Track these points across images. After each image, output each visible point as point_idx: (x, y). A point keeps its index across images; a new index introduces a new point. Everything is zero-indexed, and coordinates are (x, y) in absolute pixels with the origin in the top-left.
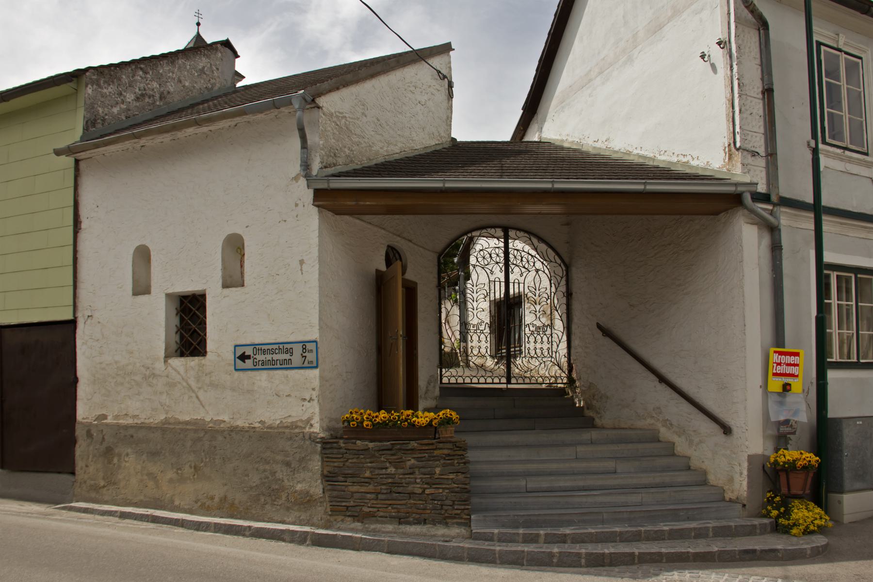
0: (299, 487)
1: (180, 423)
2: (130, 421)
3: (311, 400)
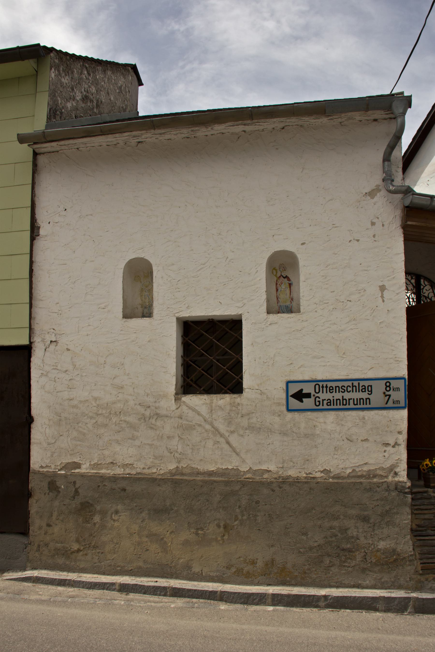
0: (382, 545)
1: (199, 473)
2: (119, 471)
3: (396, 444)
